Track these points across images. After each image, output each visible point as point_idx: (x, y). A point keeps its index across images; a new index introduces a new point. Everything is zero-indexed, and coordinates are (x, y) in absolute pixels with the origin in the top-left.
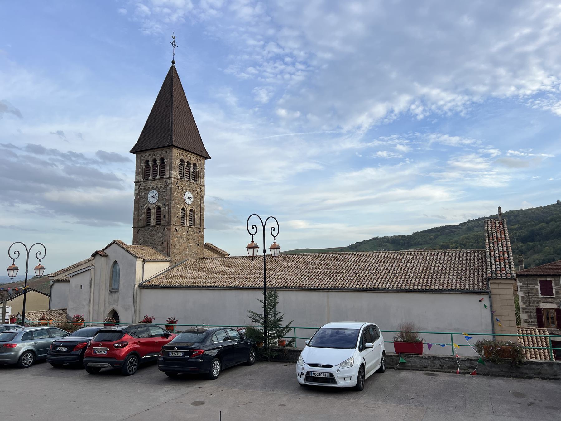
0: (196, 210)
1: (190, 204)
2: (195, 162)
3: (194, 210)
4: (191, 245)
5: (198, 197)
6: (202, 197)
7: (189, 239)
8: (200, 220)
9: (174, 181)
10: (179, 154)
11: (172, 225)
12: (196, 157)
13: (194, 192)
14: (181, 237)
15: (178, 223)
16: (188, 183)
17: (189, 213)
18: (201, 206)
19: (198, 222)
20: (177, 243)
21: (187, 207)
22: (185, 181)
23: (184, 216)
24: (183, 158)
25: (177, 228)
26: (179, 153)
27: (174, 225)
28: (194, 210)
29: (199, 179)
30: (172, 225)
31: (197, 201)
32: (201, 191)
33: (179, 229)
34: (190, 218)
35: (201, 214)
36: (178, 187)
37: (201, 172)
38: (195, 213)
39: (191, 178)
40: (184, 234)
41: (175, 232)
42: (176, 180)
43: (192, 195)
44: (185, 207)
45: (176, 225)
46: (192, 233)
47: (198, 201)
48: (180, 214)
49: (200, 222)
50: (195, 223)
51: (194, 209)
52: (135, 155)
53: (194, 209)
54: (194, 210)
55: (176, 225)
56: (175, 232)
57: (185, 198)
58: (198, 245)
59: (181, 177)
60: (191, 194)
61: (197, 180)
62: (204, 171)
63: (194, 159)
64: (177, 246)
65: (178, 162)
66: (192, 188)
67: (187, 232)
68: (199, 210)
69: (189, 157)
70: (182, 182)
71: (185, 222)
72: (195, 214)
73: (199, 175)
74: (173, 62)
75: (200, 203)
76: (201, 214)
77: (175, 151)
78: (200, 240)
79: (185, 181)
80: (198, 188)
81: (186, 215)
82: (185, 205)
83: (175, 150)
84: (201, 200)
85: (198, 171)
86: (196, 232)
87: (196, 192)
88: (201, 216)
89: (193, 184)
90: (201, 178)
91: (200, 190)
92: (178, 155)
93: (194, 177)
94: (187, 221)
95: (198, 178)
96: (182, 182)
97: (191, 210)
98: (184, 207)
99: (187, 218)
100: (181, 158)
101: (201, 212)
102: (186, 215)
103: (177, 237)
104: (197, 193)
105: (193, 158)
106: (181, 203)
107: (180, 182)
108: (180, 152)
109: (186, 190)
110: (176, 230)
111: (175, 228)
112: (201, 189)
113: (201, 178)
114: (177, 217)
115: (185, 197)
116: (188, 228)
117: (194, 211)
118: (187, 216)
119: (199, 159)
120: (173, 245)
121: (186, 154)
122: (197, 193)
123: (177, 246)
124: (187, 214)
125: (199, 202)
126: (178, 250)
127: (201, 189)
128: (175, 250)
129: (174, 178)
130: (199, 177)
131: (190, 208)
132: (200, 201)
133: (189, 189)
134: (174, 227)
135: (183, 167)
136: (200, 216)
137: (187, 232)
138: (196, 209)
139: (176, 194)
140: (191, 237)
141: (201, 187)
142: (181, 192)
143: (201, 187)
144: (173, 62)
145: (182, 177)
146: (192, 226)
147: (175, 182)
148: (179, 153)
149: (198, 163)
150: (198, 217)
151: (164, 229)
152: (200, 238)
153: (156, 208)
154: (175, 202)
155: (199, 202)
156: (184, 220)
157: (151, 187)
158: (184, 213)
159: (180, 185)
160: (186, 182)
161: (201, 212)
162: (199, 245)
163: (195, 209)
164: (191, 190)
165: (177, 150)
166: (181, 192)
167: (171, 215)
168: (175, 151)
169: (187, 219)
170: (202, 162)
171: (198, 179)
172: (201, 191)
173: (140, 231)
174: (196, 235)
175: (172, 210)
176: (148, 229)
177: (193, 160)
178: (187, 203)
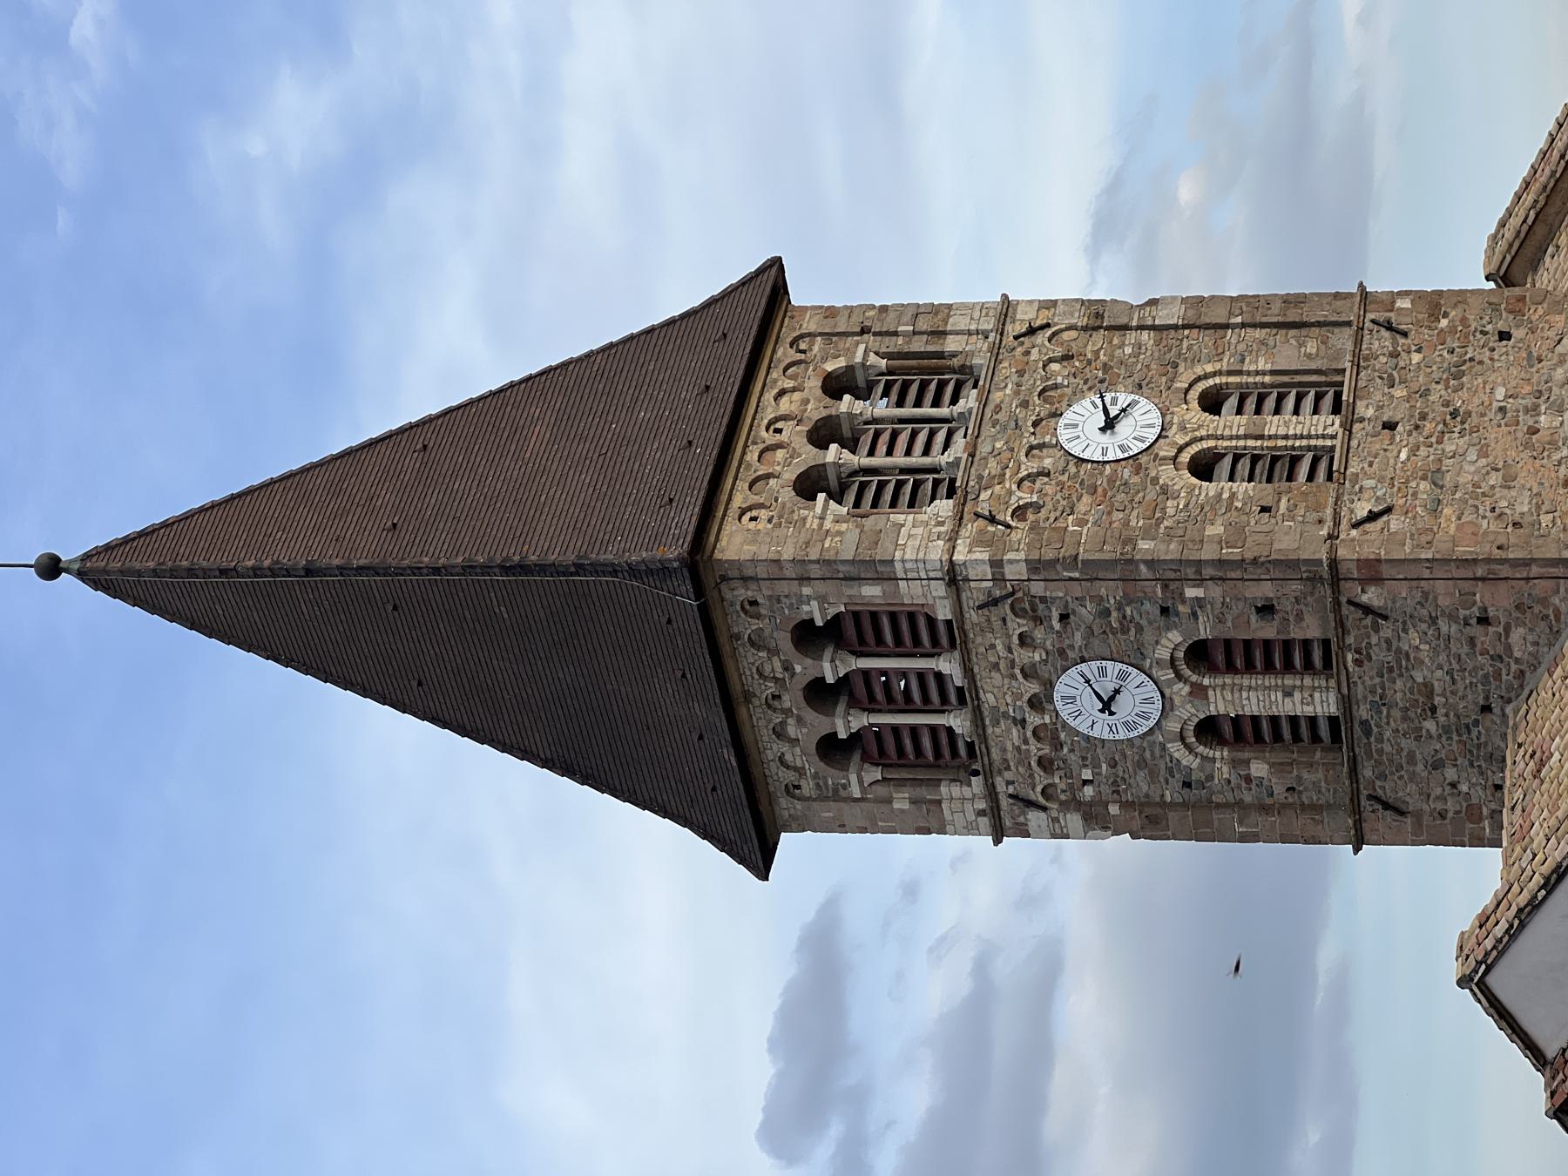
0: (1209, 368)
1: (1155, 417)
2: (814, 384)
3: (1206, 376)
4: (1500, 393)
5: (1097, 353)
6: (1099, 316)
7: (1454, 414)
8: (1292, 332)
9: (980, 541)
10: (761, 506)
11: (1333, 550)
12: (774, 374)
13: (1056, 387)
14: (1435, 476)
15: (1318, 508)
16: (988, 430)
17: (1230, 425)
18: (1175, 327)
19: (1311, 347)
20: (1484, 508)
21: (1181, 440)
22: (972, 455)
23: (1255, 459)
24: (790, 475)
25: (1362, 510)
26: (750, 509)
27: (1331, 537)
28: (1206, 376)
29: (952, 344)
30: (1333, 550)
32: (1048, 325)
33: (1366, 495)
34: (1277, 411)
35: (1243, 325)
36: (1019, 512)
37: (896, 334)
38: (1230, 373)
39: (944, 411)
40: (1414, 452)
41: (1393, 527)
42: (970, 528)
43: (1086, 403)
44: (1181, 449)
45: (1337, 522)
46: (1399, 392)
47: (1128, 350)
48: (1242, 488)
49: (1312, 325)
50: (1317, 372)
51: (1199, 379)
52: (785, 837)
53: (1199, 379)
54: (1211, 382)
55: (1337, 522)
56: (1395, 522)
57: (1110, 457)
58: (1504, 336)
59: (943, 489)
60: (1076, 408)
61: (956, 362)
62: (884, 309)
63: (794, 390)
64: (1511, 505)
65: (822, 518)
66: (1025, 404)
67: (1390, 426)
68: (1207, 338)
69: (779, 431)
70: (980, 477)
71: (1309, 448)
72: (1240, 373)
73: (919, 345)
74: (50, 568)
75: (1145, 335)
76: (1243, 325)
77: (738, 540)
78: (1464, 320)
79: (972, 455)
80: (1027, 353)
81: (1251, 443)
82: (1166, 450)
83: (723, 542)
84: (1125, 328)
85: (889, 356)
86: (1394, 355)
87: (1055, 367)
88: (1254, 326)
89: (997, 396)
90: (944, 333)
91: (1041, 338)
92: (763, 514)
93: (933, 386)
94: (1295, 437)
95: (940, 355)
96: (980, 477)
97: (1212, 403)
98: (1185, 457)
99: (1270, 437)
100: (788, 495)
101: (1226, 326)
102: (1251, 443)
103: (1435, 509)
104: (1067, 358)
105: (785, 400)
106: (1155, 481)
107: (984, 495)
108: (738, 501)
109: (1041, 446)
110: (1372, 517)
111: (1356, 526)
112: (1032, 331)
113: (944, 333)
114: (1264, 509)
115: (1104, 452)
116: (1357, 427)
117: (1211, 382)
118: (1261, 437)
119: (785, 353)
120: (1502, 540)
122: (1067, 358)
123: (1511, 505)
124: (1246, 437)
125: (1138, 346)
126: (1548, 495)
127: (1032, 331)
128: (1546, 520)
129: (952, 539)
130: (931, 348)
131: (1194, 414)
132: (1131, 337)
133: (1035, 424)
134: (1354, 532)
135: (855, 473)
136: (1259, 333)
137: (1390, 426)
139: (1081, 523)
140: (1438, 392)
141: (1013, 329)
142: (1061, 485)
143: (1013, 329)
144: (50, 568)
145: (936, 483)
146: (1338, 395)
147: (981, 532)
148: (750, 509)
149: (825, 359)
150: (1263, 343)
151: (1367, 610)
152: (1444, 323)
153: (1194, 678)
154: (1147, 534)
155: (1138, 346)
156: (1295, 461)
157: (1034, 719)
158: (1237, 458)
159: (1010, 493)
160: (983, 449)
161: (1226, 326)
162: (1501, 326)
163: (1199, 370)
164: (1039, 408)
165: (730, 526)
166: (1061, 485)
167: (1249, 556)
168: (738, 540)
169: (1286, 437)
170: (812, 328)
171: (954, 355)
172: (1048, 325)
173: (1389, 796)
174: (1416, 358)
175: (1208, 553)
176: (1368, 733)
177: (797, 396)
178: (1151, 435)
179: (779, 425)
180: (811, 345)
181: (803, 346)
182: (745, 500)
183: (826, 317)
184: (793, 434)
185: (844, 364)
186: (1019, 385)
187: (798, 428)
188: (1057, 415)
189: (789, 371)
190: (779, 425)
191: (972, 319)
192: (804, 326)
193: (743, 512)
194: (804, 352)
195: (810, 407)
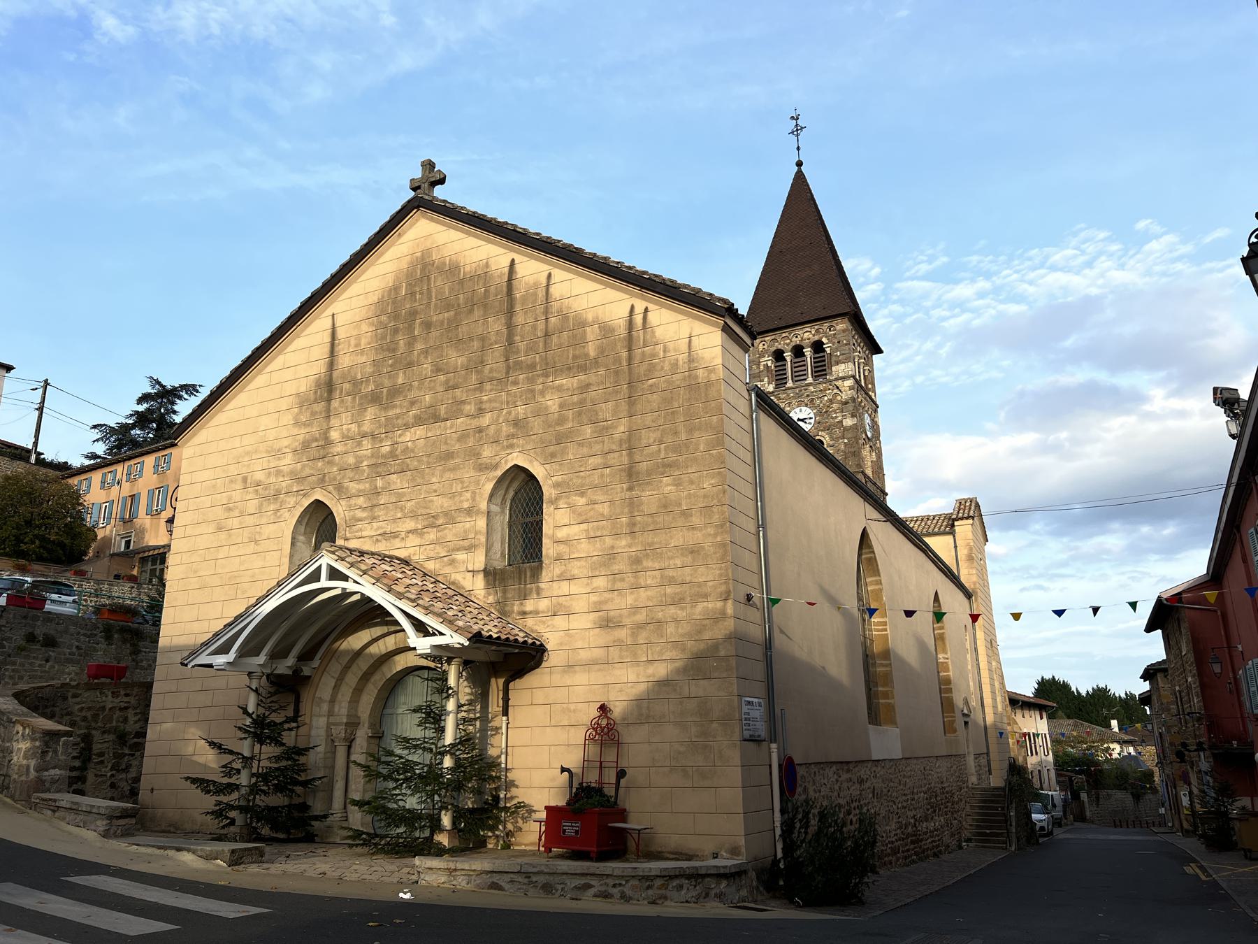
2: (816, 338)
12: (816, 327)
16: (797, 391)
24: (780, 347)
31: (832, 418)
66: (808, 396)
91: (836, 391)
100: (773, 349)
105: (808, 333)
121: (784, 335)
125: (836, 417)
127: (838, 388)
138: (830, 434)
141: (839, 383)
143: (839, 383)
144: (799, 164)
155: (836, 417)
160: (789, 392)
184: (796, 341)
186: (816, 392)
188: (806, 406)
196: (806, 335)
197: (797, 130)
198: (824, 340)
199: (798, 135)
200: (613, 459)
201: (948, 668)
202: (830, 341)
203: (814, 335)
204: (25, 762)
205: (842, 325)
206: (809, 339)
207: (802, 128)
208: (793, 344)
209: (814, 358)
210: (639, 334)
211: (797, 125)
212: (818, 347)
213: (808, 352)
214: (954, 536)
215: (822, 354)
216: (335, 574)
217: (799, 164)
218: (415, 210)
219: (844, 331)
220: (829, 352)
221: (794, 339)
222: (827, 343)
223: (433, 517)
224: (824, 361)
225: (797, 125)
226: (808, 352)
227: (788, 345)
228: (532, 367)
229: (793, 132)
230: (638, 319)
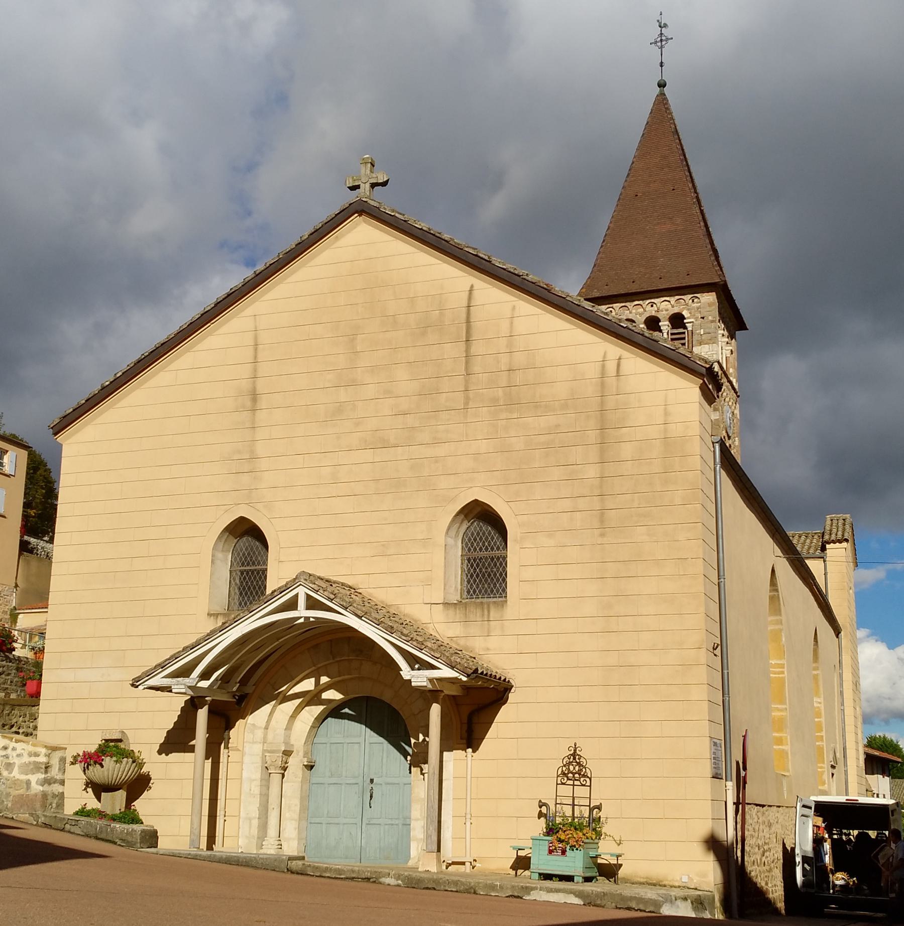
2: (676, 310)
105: (667, 303)
108: (614, 305)
144: (662, 85)
179: (654, 305)
180: (697, 303)
181: (695, 300)
182: (617, 307)
183: (708, 304)
184: (651, 311)
185: (686, 316)
187: (654, 312)
189: (682, 300)
190: (654, 305)
191: (707, 352)
192: (703, 298)
193: (612, 308)
194: (693, 301)
195: (664, 312)
196: (665, 307)
197: (661, 40)
198: (685, 313)
199: (662, 47)
200: (582, 503)
201: (820, 714)
202: (692, 316)
203: (673, 307)
204: (23, 777)
205: (709, 298)
206: (667, 310)
207: (667, 39)
208: (647, 315)
209: (672, 334)
210: (611, 381)
211: (661, 34)
212: (677, 320)
213: (665, 325)
214: (824, 561)
215: (681, 330)
216: (312, 604)
217: (662, 85)
218: (356, 215)
219: (710, 305)
220: (690, 329)
221: (649, 308)
222: (689, 318)
223: (383, 545)
224: (684, 338)
225: (661, 34)
226: (665, 325)
227: (641, 314)
228: (494, 401)
229: (656, 42)
230: (611, 367)
